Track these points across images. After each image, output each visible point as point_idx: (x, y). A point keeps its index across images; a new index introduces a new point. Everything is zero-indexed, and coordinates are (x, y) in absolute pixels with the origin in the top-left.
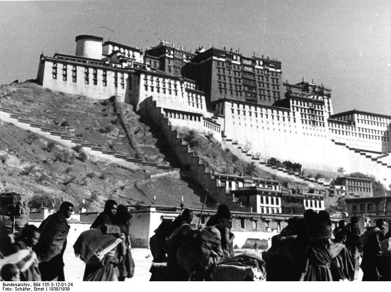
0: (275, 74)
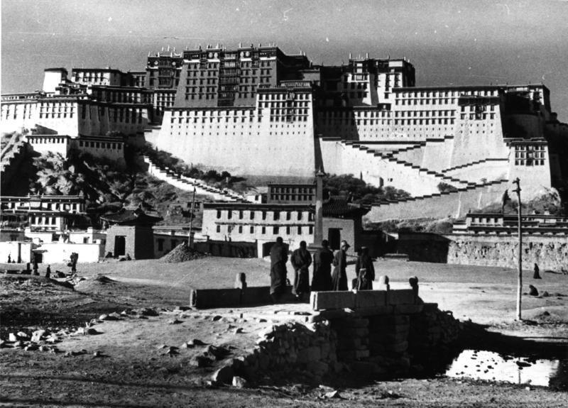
0: (266, 64)
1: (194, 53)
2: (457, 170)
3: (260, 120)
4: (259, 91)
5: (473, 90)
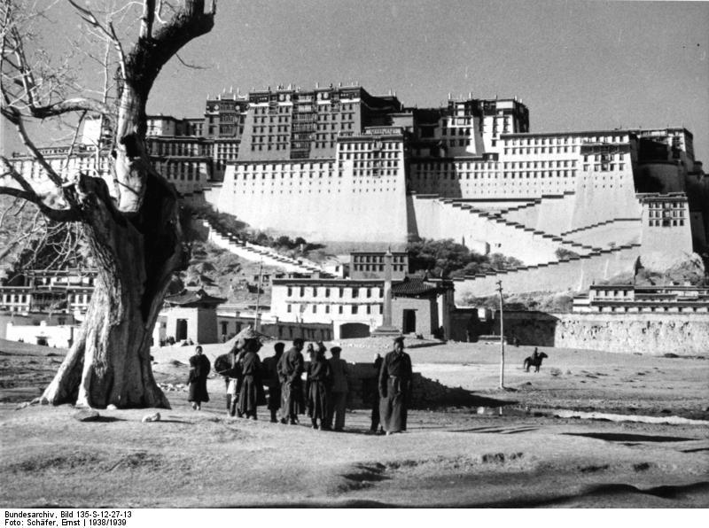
1: (263, 94)
2: (579, 232)
3: (340, 174)
4: (339, 140)
5: (598, 135)
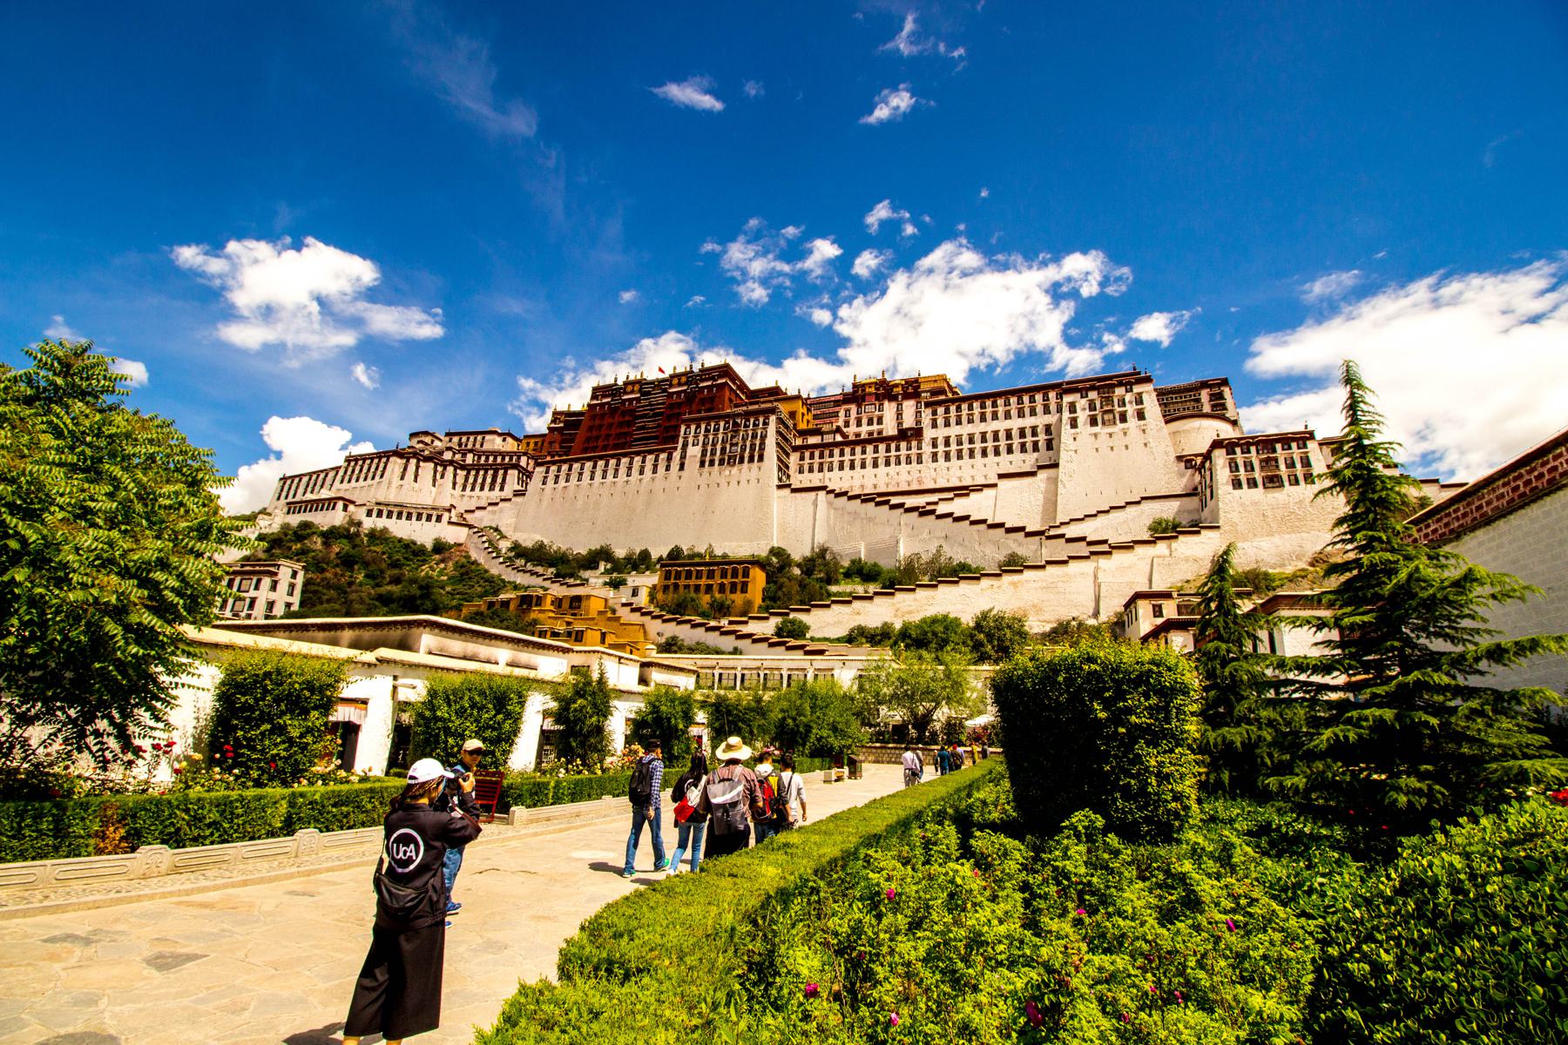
3: (682, 467)
4: (684, 421)
